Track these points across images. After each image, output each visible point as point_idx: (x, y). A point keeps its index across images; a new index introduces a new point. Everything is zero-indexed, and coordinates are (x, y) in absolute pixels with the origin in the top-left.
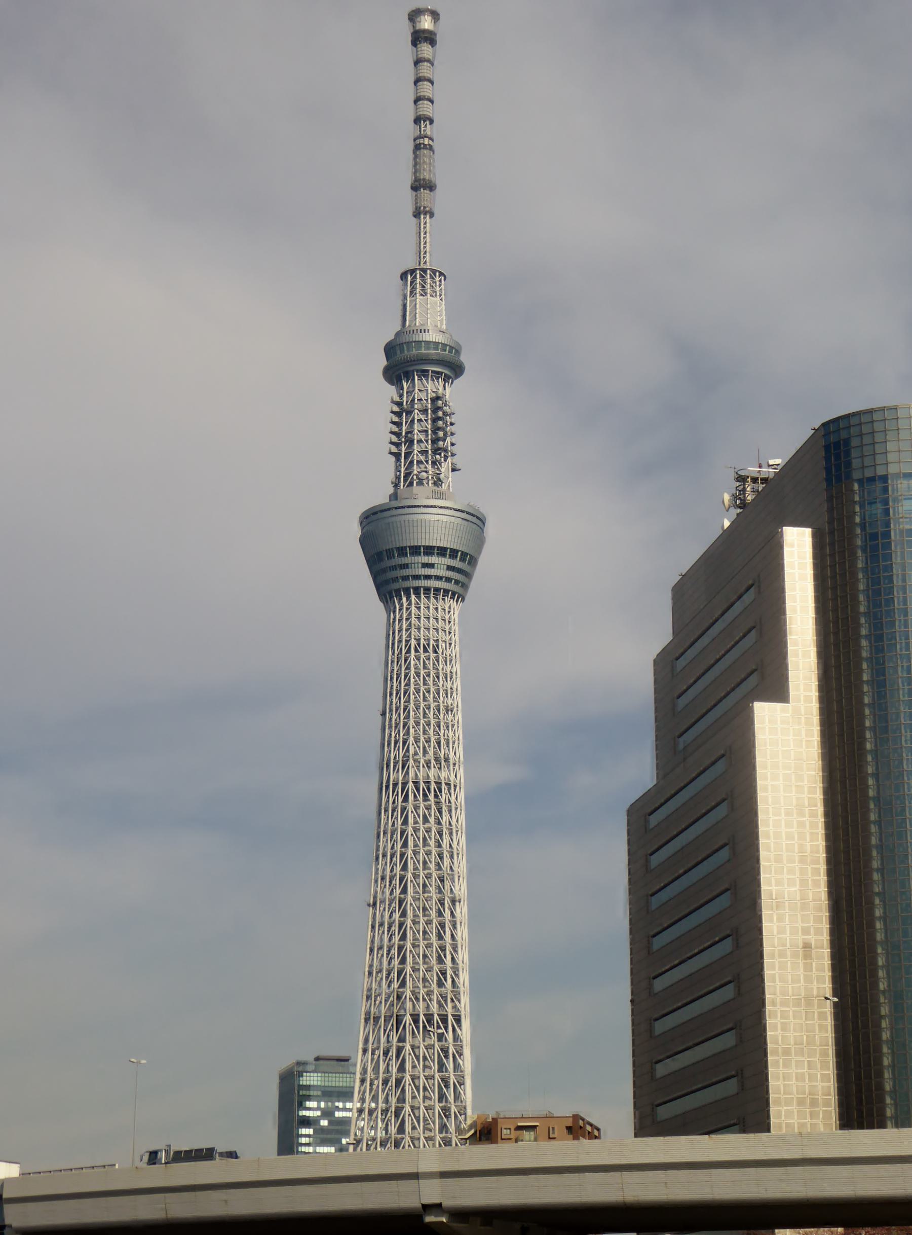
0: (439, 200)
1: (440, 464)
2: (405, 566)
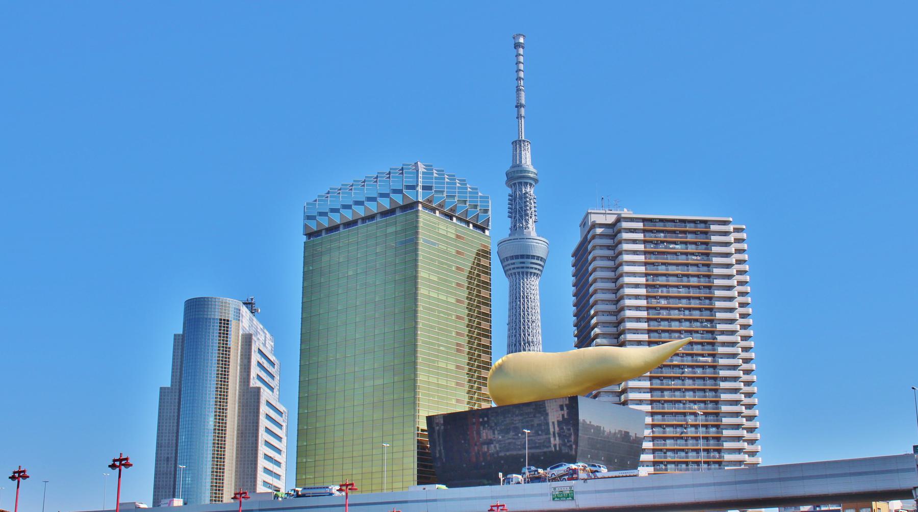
1: (528, 220)
2: (514, 263)
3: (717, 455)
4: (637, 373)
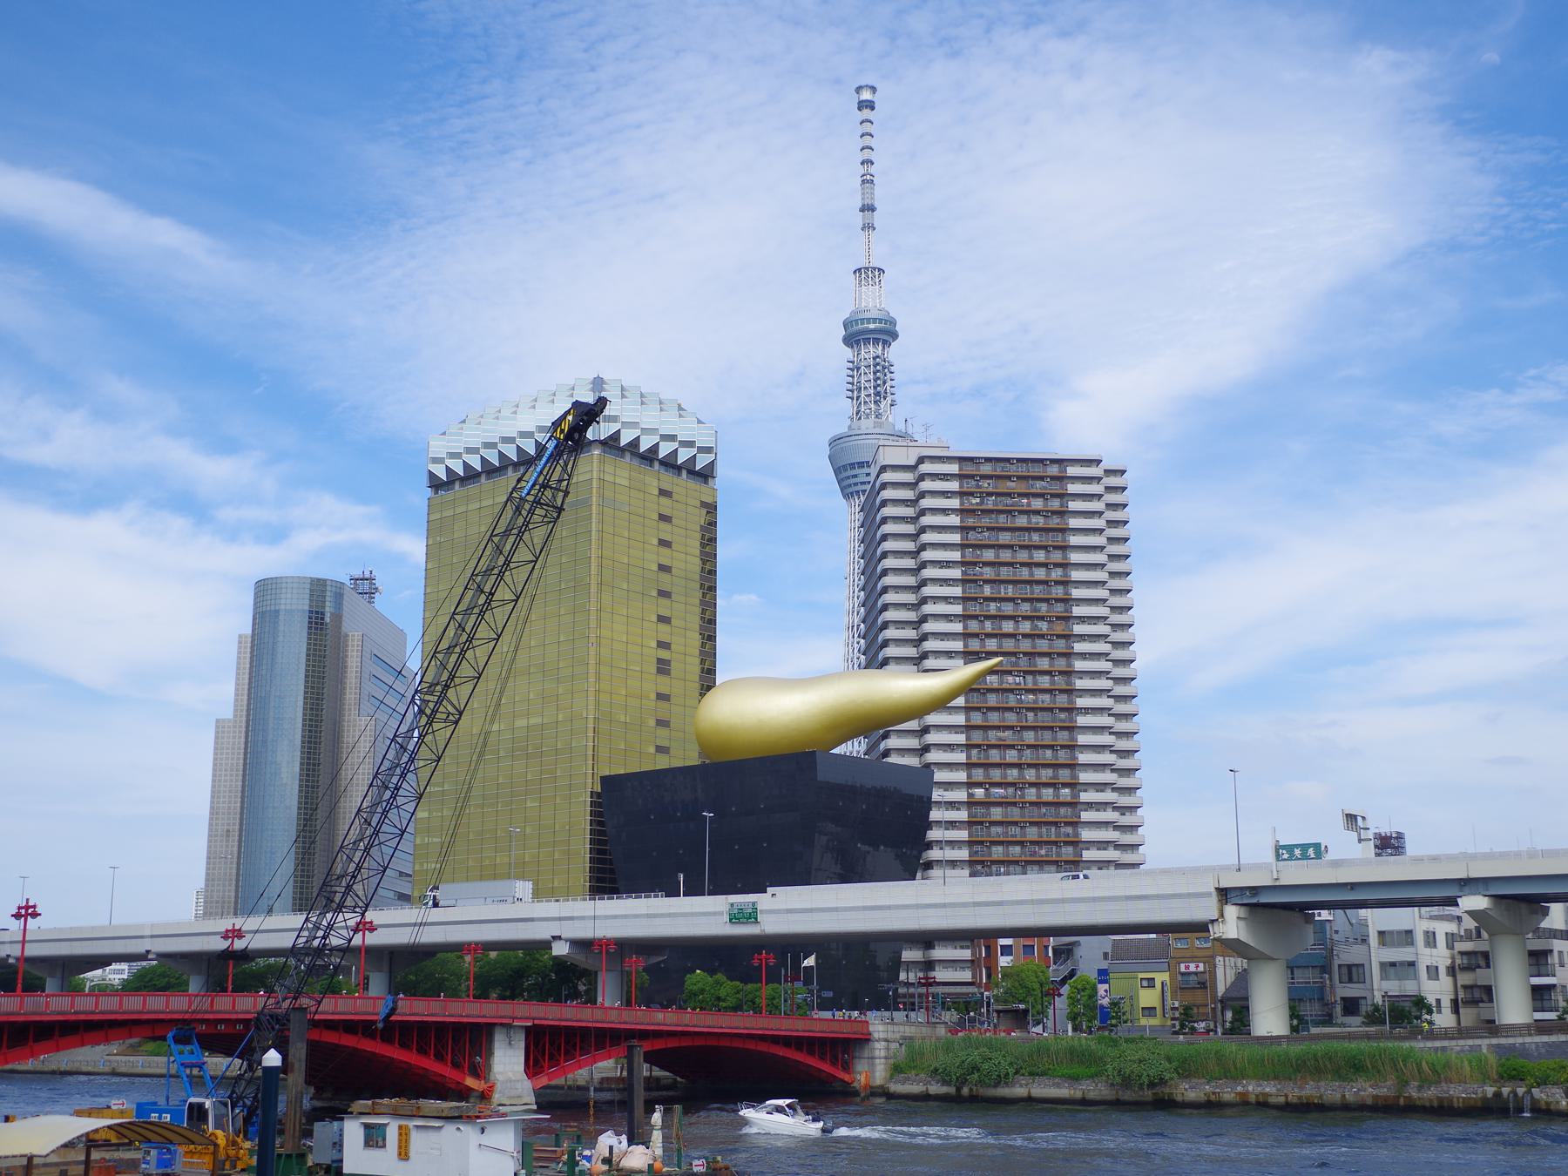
0: (878, 218)
2: (855, 476)
3: (1069, 830)
4: (940, 703)
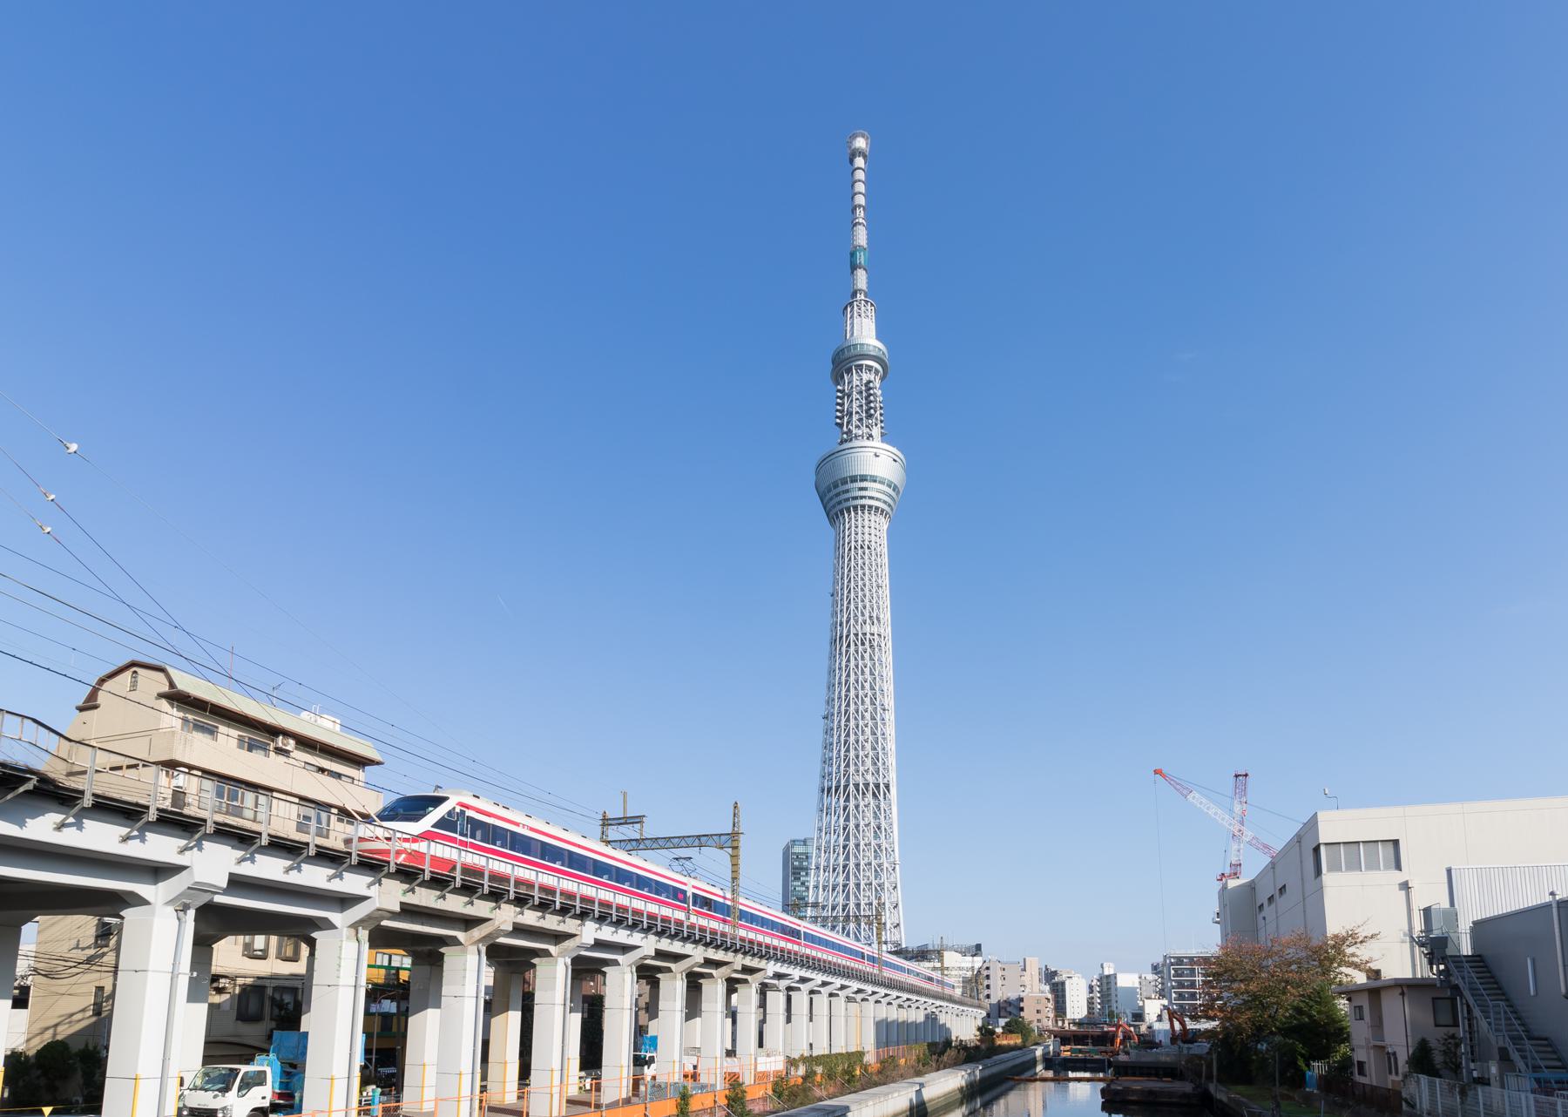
2: (847, 491)
